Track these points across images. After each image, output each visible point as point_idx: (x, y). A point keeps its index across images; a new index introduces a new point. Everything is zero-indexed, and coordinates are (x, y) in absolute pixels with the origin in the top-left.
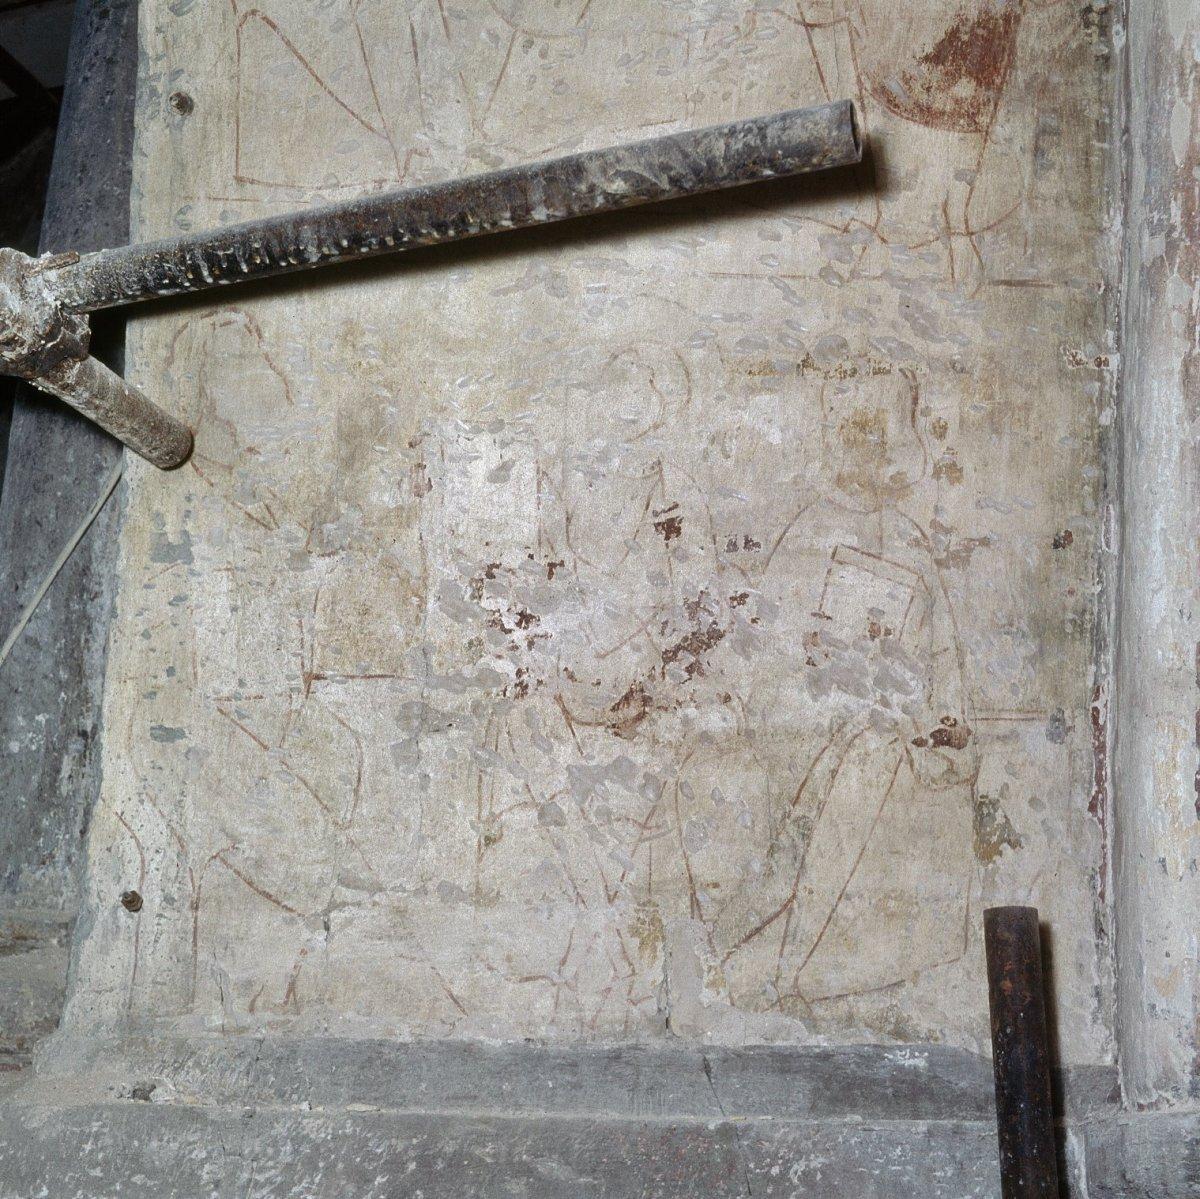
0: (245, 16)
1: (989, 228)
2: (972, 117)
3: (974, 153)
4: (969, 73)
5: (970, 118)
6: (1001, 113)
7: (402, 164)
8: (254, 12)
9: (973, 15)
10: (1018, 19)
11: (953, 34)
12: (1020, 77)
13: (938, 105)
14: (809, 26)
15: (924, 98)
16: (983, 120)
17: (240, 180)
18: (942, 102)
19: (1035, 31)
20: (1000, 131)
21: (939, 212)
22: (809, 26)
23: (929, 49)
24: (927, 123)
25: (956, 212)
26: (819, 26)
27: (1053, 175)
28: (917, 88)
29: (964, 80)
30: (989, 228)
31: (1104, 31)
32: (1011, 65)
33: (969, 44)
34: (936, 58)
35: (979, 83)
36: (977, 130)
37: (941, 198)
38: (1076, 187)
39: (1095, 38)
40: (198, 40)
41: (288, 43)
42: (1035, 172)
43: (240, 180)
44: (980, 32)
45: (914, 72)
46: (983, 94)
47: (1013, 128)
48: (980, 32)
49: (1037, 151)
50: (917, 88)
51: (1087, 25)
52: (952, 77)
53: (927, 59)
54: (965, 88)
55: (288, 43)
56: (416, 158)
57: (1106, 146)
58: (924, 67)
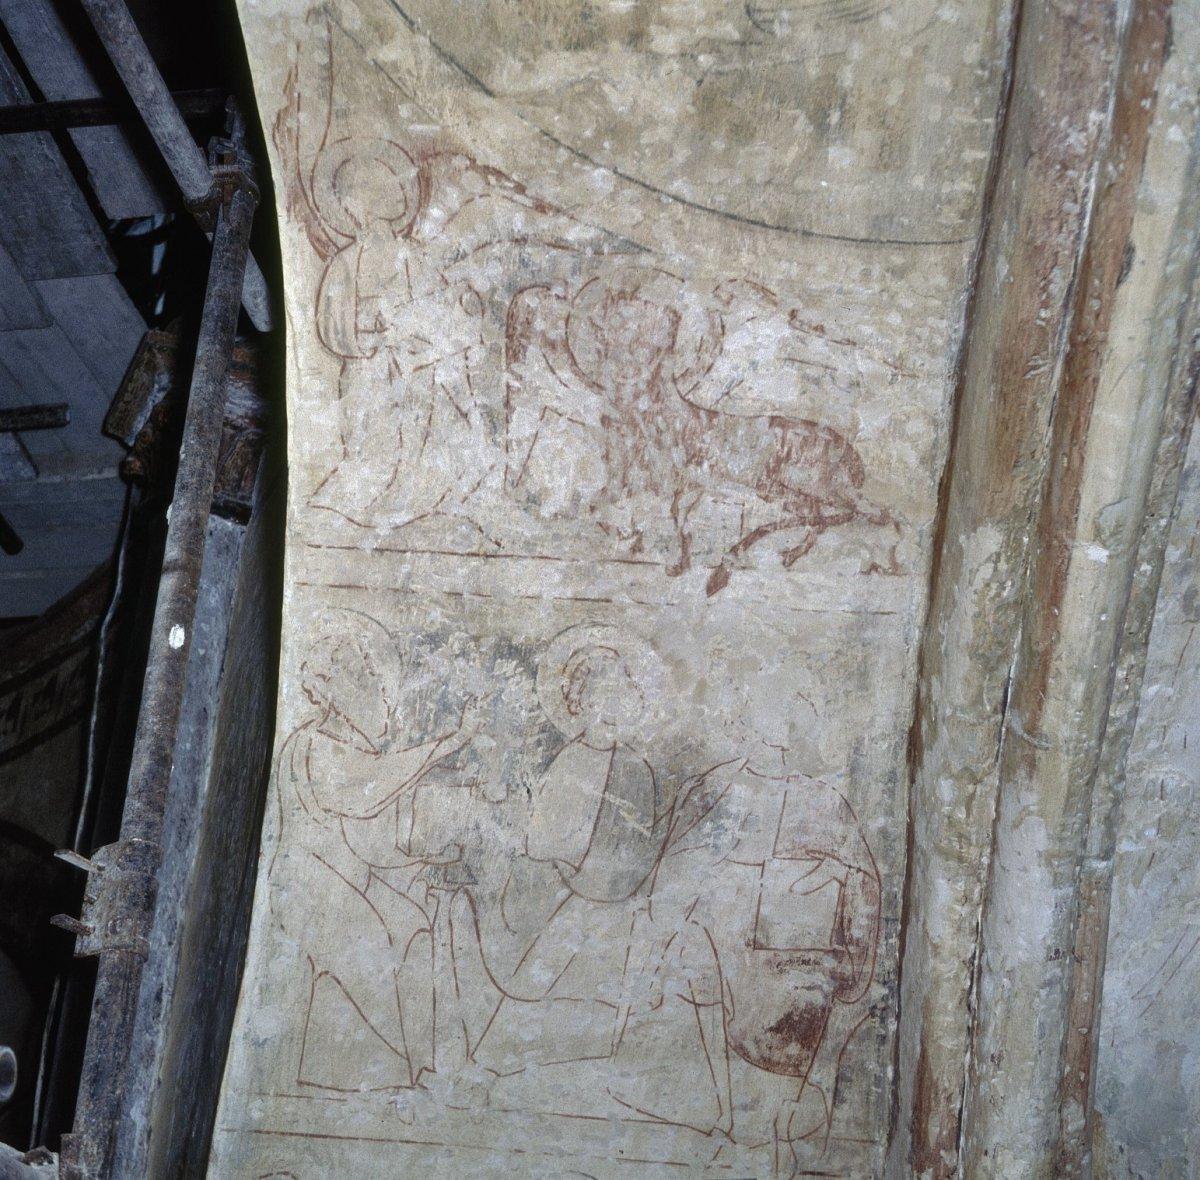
0: (320, 975)
1: (802, 1138)
2: (797, 1067)
3: (797, 1090)
4: (797, 1040)
5: (797, 1070)
6: (816, 1065)
7: (414, 1077)
8: (327, 973)
9: (802, 1005)
10: (830, 1011)
11: (789, 1016)
12: (829, 1044)
13: (775, 1058)
14: (697, 1005)
15: (767, 1053)
16: (804, 1069)
17: (300, 1083)
18: (777, 1056)
19: (840, 1018)
20: (814, 1077)
21: (771, 1125)
22: (697, 1005)
23: (773, 1024)
24: (767, 1069)
25: (782, 1125)
26: (704, 1005)
27: (846, 1106)
28: (763, 1046)
29: (793, 1044)
30: (802, 1138)
31: (883, 1020)
32: (823, 1037)
33: (800, 1022)
34: (777, 1029)
35: (803, 1046)
36: (799, 1076)
37: (774, 1117)
38: (860, 1114)
39: (877, 1025)
40: (284, 988)
41: (347, 994)
42: (834, 1103)
43: (300, 1083)
44: (805, 1015)
45: (763, 1037)
46: (805, 1053)
47: (823, 1075)
48: (805, 1015)
49: (836, 1092)
50: (763, 1046)
51: (873, 1015)
52: (786, 1041)
53: (771, 1029)
54: (794, 1049)
55: (347, 994)
56: (425, 1072)
57: (880, 1090)
58: (769, 1035)
